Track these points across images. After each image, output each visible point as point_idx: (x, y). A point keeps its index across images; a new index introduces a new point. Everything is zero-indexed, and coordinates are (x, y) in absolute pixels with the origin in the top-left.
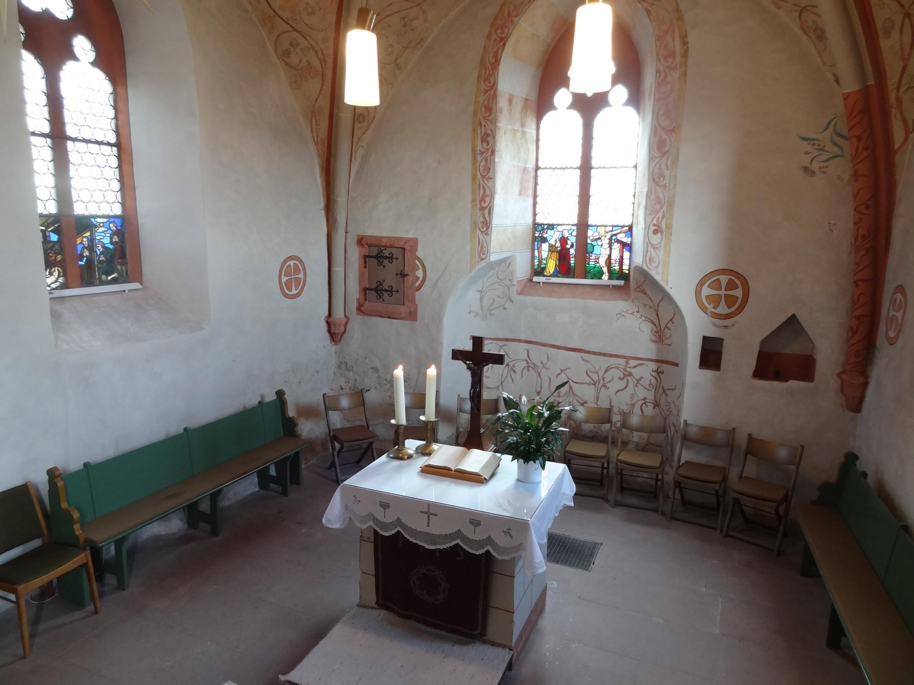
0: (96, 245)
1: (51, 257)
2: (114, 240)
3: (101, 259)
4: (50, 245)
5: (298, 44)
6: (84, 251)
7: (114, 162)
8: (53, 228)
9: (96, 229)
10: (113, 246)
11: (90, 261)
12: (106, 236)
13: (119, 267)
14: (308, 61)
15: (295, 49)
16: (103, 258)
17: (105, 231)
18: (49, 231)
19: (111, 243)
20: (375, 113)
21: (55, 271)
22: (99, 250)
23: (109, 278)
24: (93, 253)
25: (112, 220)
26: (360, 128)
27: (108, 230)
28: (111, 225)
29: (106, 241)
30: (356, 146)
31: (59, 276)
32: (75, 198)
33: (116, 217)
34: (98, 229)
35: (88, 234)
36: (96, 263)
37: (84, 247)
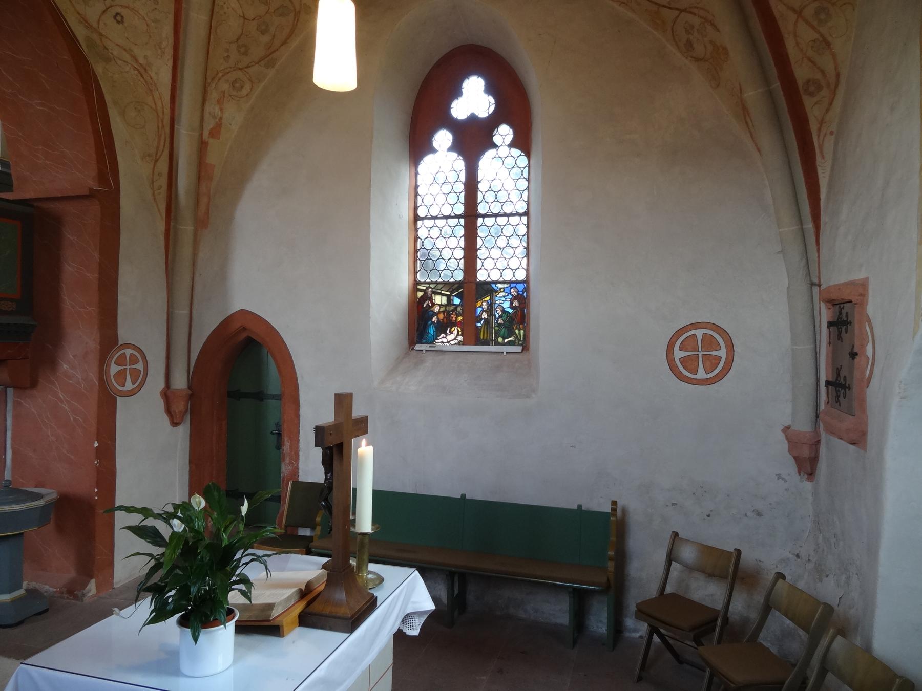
0: (495, 309)
2: (514, 305)
3: (499, 322)
4: (452, 308)
5: (692, 27)
8: (457, 293)
11: (487, 322)
13: (517, 331)
14: (711, 42)
15: (692, 34)
16: (502, 322)
17: (505, 296)
18: (453, 296)
19: (511, 307)
20: (836, 68)
21: (455, 330)
22: (498, 314)
23: (506, 341)
24: (491, 317)
25: (513, 285)
26: (816, 104)
27: (508, 296)
28: (512, 290)
29: (506, 305)
30: (819, 136)
31: (458, 334)
32: (479, 266)
33: (518, 282)
35: (488, 299)
37: (483, 310)
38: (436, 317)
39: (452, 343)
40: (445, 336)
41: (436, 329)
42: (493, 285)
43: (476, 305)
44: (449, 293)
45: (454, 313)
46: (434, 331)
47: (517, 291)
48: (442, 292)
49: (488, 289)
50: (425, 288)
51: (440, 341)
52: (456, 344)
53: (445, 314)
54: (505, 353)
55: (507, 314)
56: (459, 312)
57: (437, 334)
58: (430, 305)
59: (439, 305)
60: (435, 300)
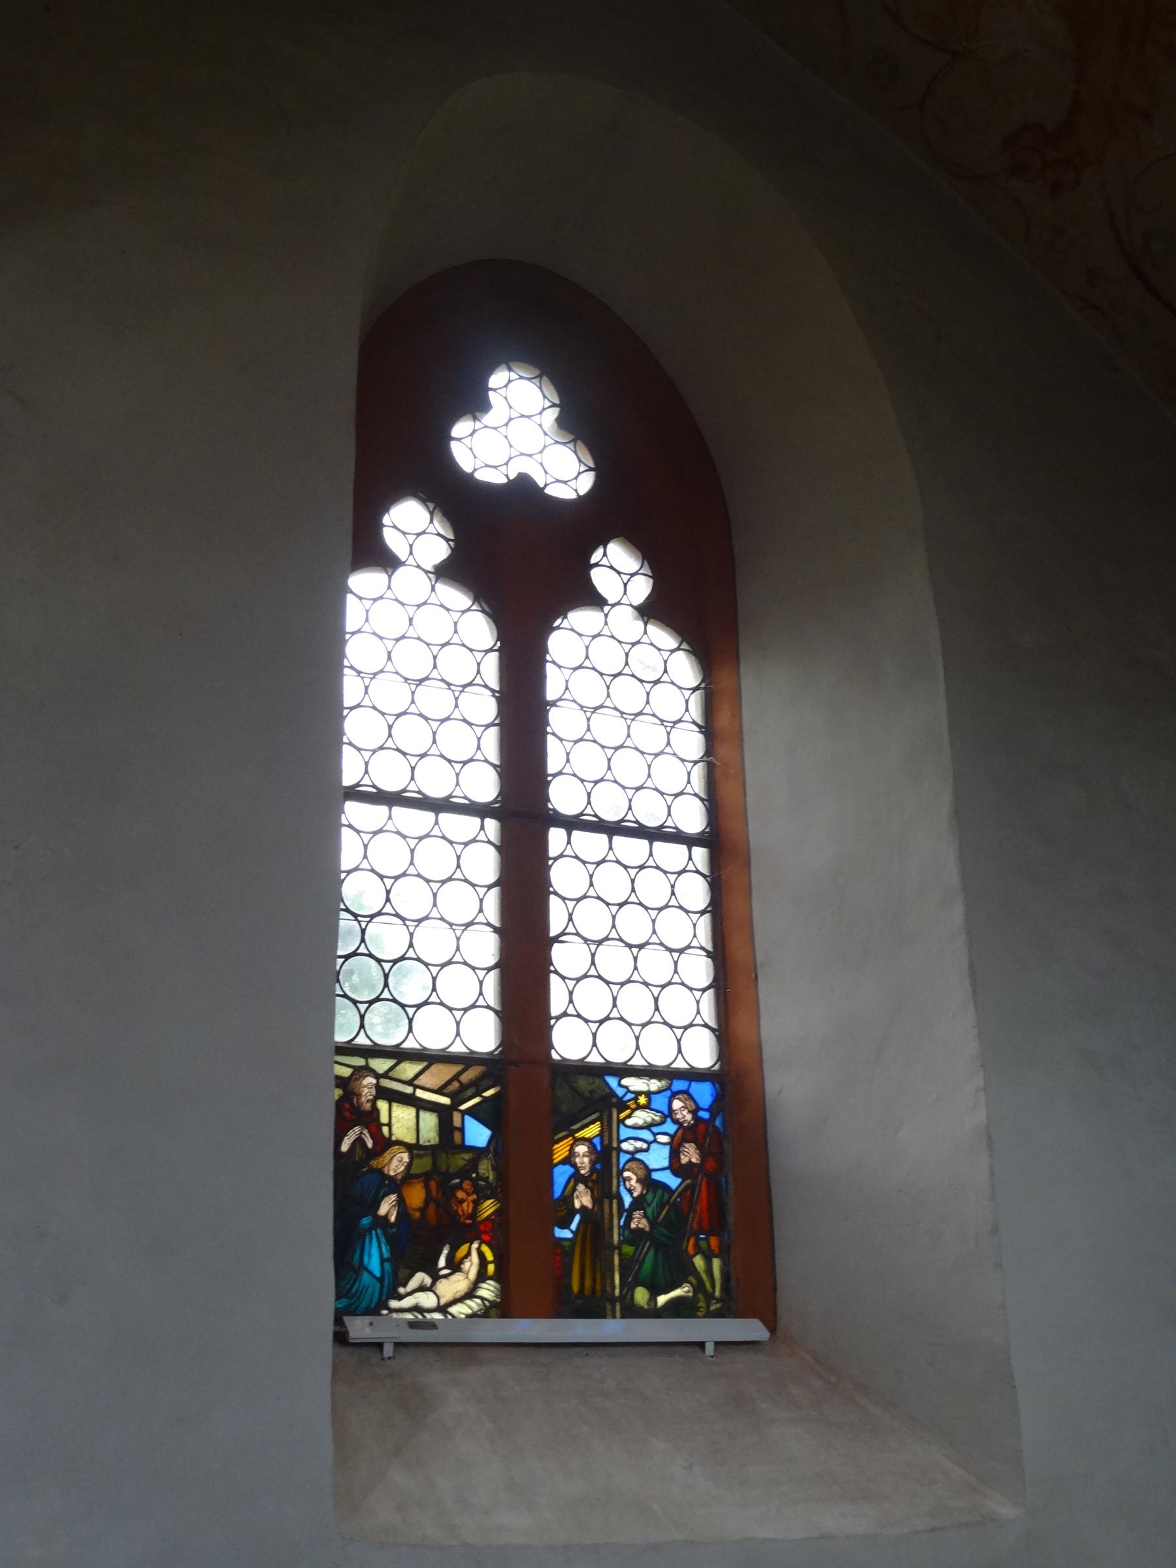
0: (620, 1172)
1: (462, 1201)
2: (684, 1160)
3: (633, 1226)
4: (462, 1159)
6: (574, 1190)
7: (696, 893)
8: (477, 1100)
9: (622, 1115)
10: (679, 1180)
11: (594, 1222)
12: (655, 1141)
13: (699, 1262)
18: (464, 1113)
19: (675, 1166)
21: (469, 1254)
22: (630, 1191)
23: (662, 1300)
24: (606, 1202)
25: (679, 1085)
27: (662, 1123)
28: (677, 1104)
29: (657, 1158)
31: (482, 1276)
32: (557, 1002)
33: (693, 1075)
34: (629, 1116)
35: (593, 1131)
36: (616, 1237)
37: (577, 1177)
38: (393, 1197)
39: (460, 1310)
40: (428, 1281)
41: (392, 1251)
42: (612, 1081)
43: (551, 1153)
44: (445, 1100)
45: (467, 1185)
46: (383, 1261)
47: (692, 1106)
48: (420, 1094)
49: (592, 1092)
50: (346, 1072)
51: (407, 1302)
52: (474, 1315)
53: (433, 1184)
54: (710, 1348)
55: (659, 1192)
56: (486, 1179)
57: (395, 1273)
58: (370, 1144)
59: (409, 1147)
60: (389, 1125)
